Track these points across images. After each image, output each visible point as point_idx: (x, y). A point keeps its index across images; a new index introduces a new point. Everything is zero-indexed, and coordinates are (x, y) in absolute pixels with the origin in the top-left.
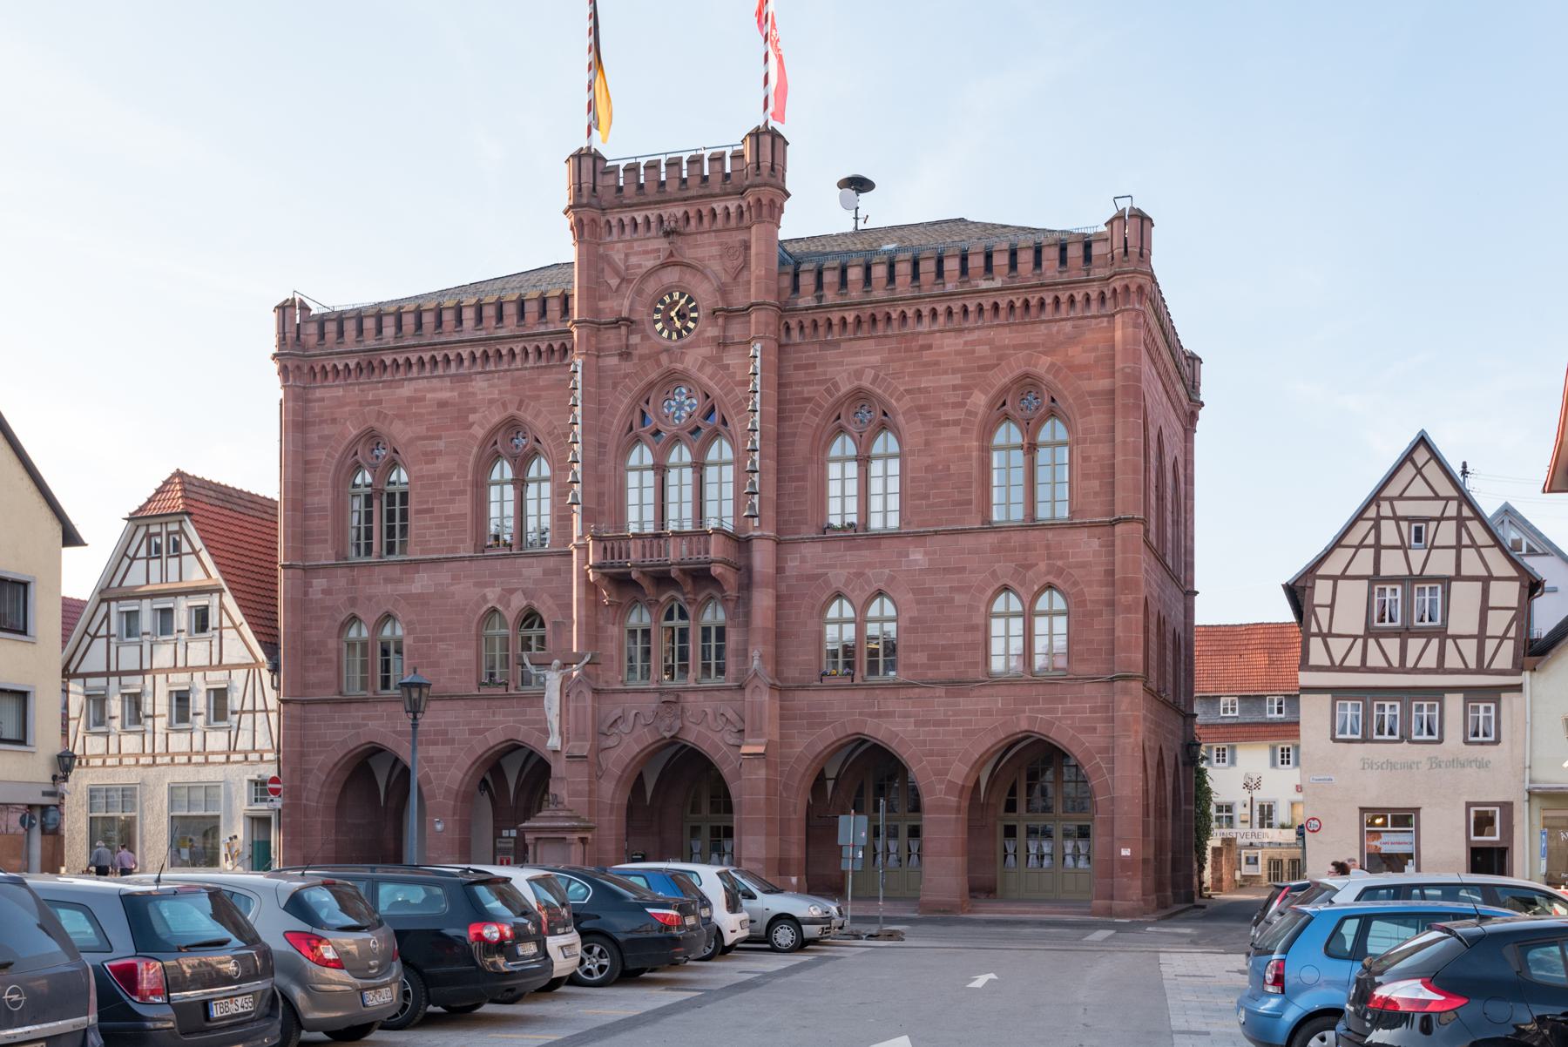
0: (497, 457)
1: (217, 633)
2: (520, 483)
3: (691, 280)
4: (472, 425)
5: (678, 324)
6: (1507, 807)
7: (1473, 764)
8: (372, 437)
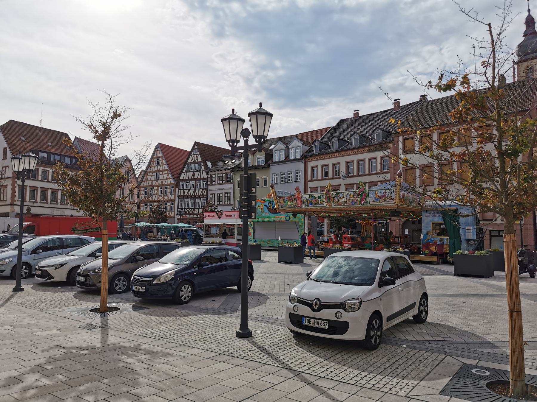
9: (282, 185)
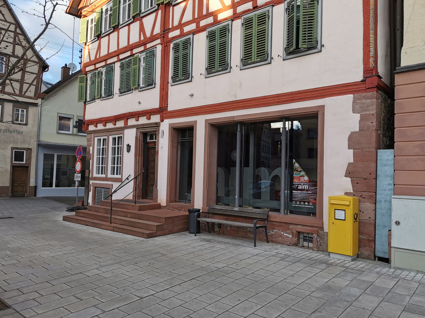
6: (29, 150)
7: (15, 132)
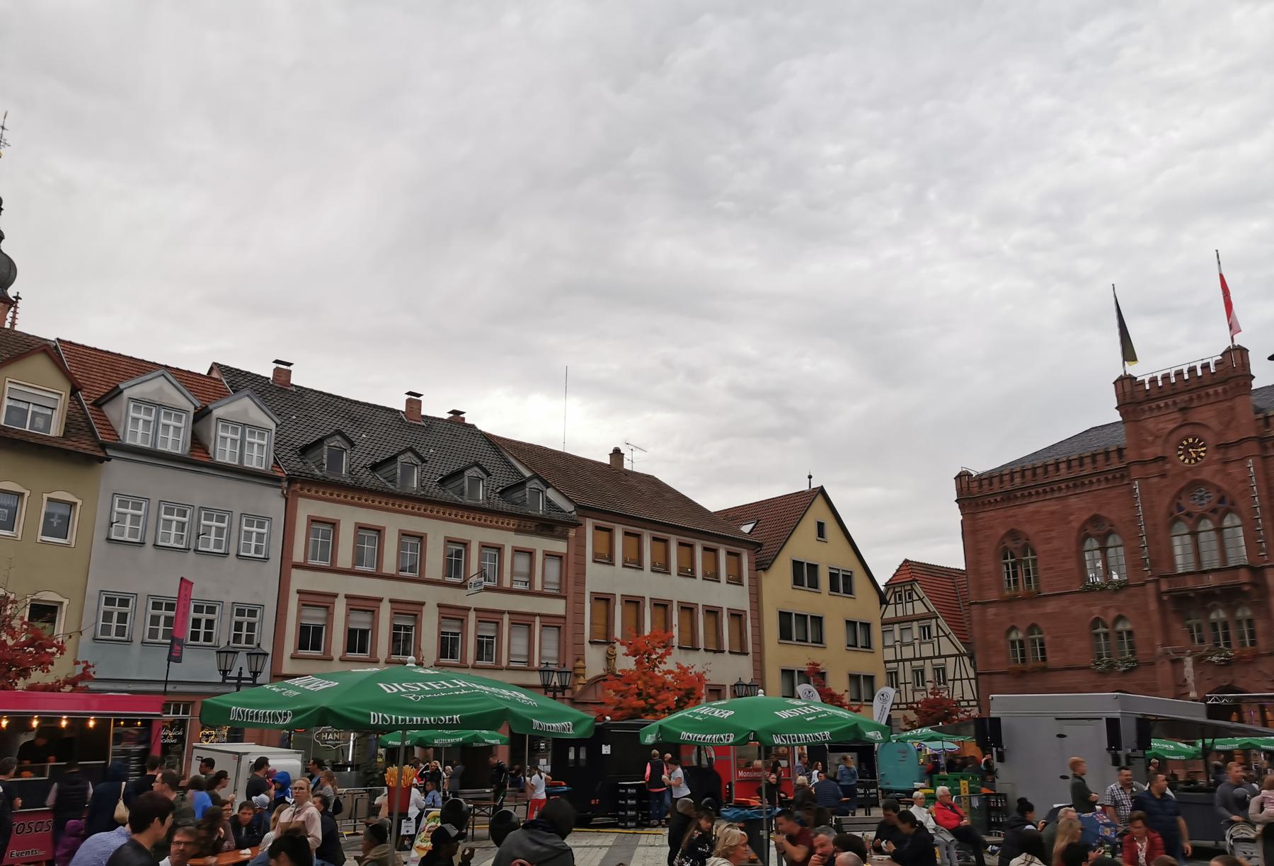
0: (1088, 536)
1: (936, 639)
2: (1104, 549)
3: (1198, 431)
4: (1070, 522)
5: (1194, 455)
8: (1013, 534)
9: (243, 563)
